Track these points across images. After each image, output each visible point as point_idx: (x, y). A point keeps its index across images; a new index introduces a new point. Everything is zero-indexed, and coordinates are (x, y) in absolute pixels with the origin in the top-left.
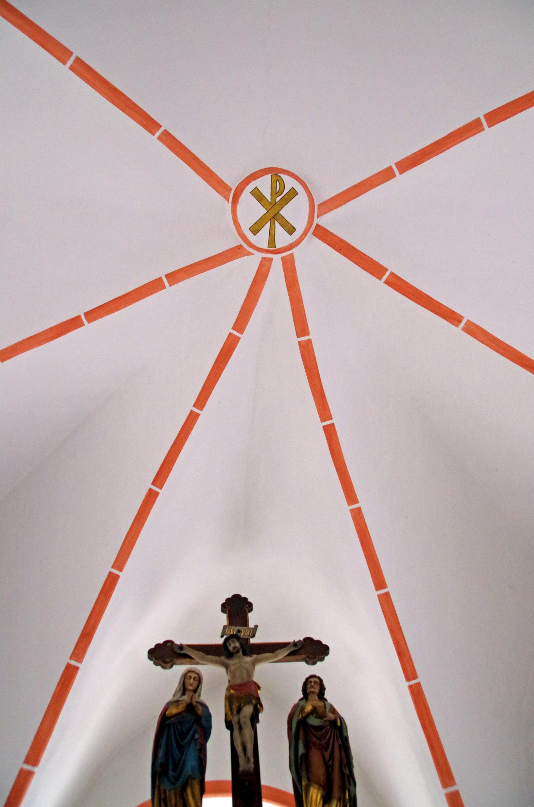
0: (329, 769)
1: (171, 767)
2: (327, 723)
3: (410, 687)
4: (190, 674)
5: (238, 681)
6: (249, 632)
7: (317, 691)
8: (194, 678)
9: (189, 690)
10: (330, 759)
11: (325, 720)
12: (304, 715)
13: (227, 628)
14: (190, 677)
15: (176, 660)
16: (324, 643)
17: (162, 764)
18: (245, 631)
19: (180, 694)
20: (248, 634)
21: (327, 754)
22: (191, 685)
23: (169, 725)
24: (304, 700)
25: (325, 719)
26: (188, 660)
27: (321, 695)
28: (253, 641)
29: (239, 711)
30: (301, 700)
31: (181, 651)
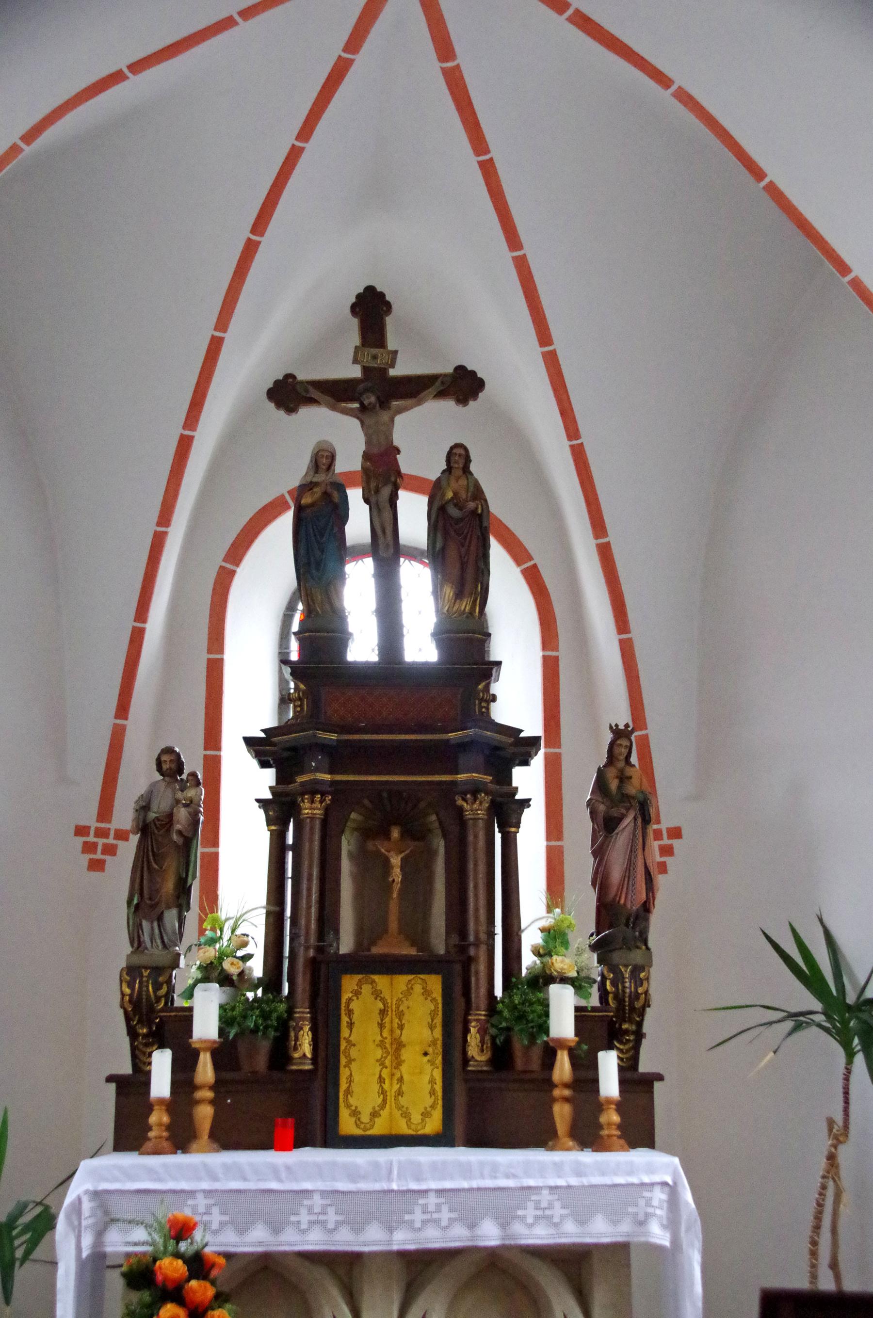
5: (375, 451)
6: (387, 357)
14: (323, 456)
16: (479, 376)
19: (312, 473)
24: (448, 473)
27: (466, 470)
28: (392, 372)
29: (377, 491)
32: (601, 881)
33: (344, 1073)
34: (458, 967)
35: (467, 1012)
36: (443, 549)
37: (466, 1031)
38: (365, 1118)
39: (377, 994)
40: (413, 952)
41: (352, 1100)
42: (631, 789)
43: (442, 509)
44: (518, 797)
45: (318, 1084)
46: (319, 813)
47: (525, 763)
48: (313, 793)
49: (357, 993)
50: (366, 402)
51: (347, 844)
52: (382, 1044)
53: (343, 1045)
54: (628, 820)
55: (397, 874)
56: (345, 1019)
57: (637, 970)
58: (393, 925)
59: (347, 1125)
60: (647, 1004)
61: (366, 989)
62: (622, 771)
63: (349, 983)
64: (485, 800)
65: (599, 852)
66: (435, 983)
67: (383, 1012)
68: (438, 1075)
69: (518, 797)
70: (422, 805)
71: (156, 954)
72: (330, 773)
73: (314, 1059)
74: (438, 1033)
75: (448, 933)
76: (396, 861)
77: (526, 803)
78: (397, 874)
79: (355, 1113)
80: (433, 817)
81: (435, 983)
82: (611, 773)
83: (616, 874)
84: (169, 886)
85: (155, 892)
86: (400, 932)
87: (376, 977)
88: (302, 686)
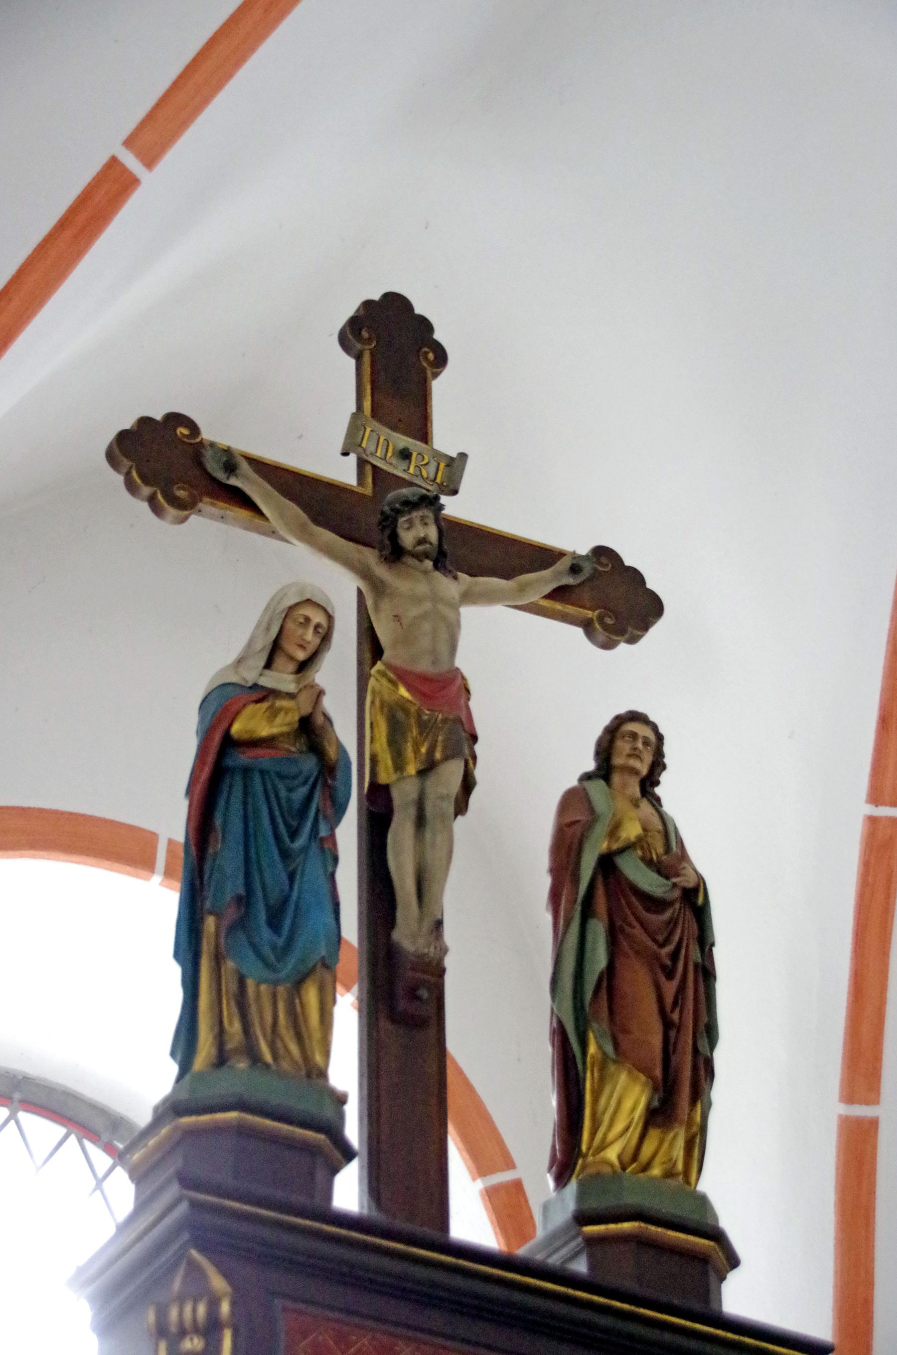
1: (262, 915)
2: (677, 893)
3: (872, 821)
4: (308, 611)
7: (644, 770)
8: (317, 626)
9: (291, 658)
10: (675, 1003)
11: (675, 885)
12: (615, 846)
13: (368, 430)
14: (307, 620)
15: (206, 505)
17: (239, 900)
18: (423, 458)
20: (432, 476)
21: (670, 988)
22: (302, 647)
23: (246, 771)
25: (675, 880)
26: (244, 514)
30: (587, 777)
31: (228, 478)
50: (407, 538)
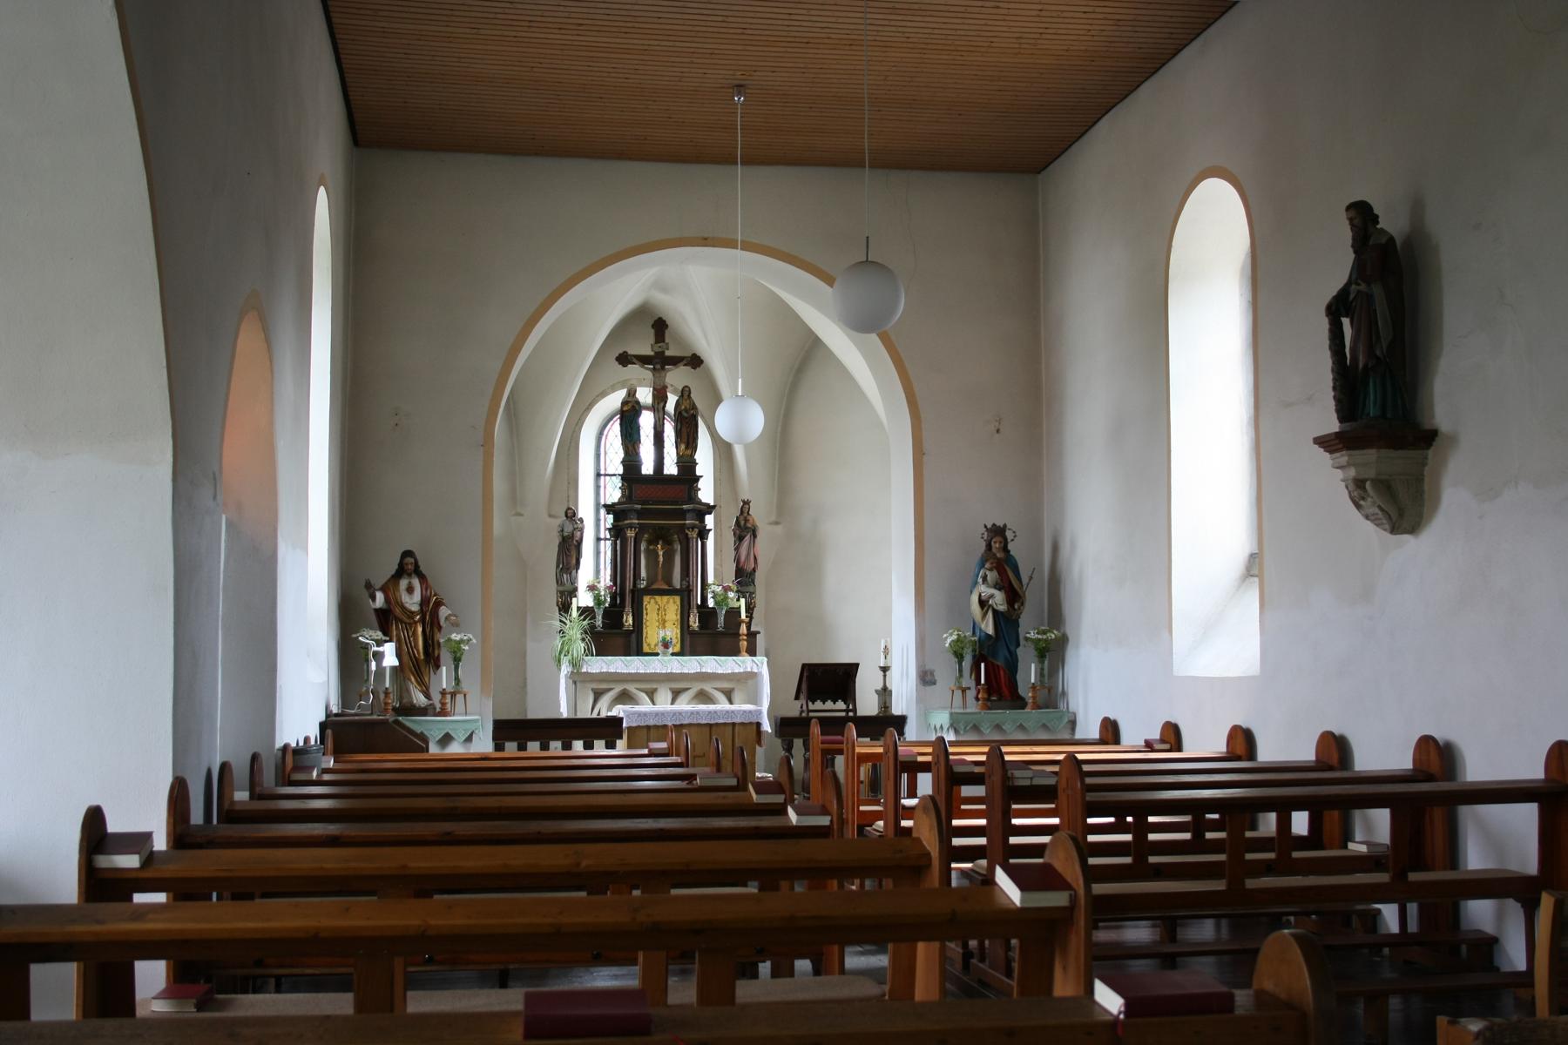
0: (688, 436)
27: (689, 396)
32: (737, 560)
33: (645, 631)
34: (686, 593)
35: (689, 610)
36: (681, 429)
37: (689, 616)
38: (652, 647)
39: (656, 603)
40: (666, 587)
41: (648, 641)
42: (749, 525)
43: (680, 413)
44: (707, 528)
45: (634, 636)
46: (633, 535)
47: (710, 513)
48: (631, 528)
49: (649, 602)
51: (643, 546)
52: (658, 621)
53: (644, 621)
54: (747, 538)
55: (661, 559)
56: (645, 612)
57: (751, 593)
58: (660, 577)
59: (646, 649)
60: (755, 606)
61: (652, 601)
62: (746, 518)
63: (646, 599)
64: (696, 530)
65: (737, 549)
66: (678, 599)
67: (659, 609)
68: (679, 631)
69: (707, 528)
70: (671, 531)
71: (568, 586)
72: (638, 519)
73: (633, 626)
74: (679, 617)
75: (681, 581)
76: (661, 553)
77: (711, 530)
78: (661, 559)
79: (649, 645)
80: (676, 536)
81: (678, 599)
82: (742, 518)
83: (743, 558)
84: (574, 561)
85: (568, 564)
86: (663, 579)
87: (657, 597)
88: (625, 484)
